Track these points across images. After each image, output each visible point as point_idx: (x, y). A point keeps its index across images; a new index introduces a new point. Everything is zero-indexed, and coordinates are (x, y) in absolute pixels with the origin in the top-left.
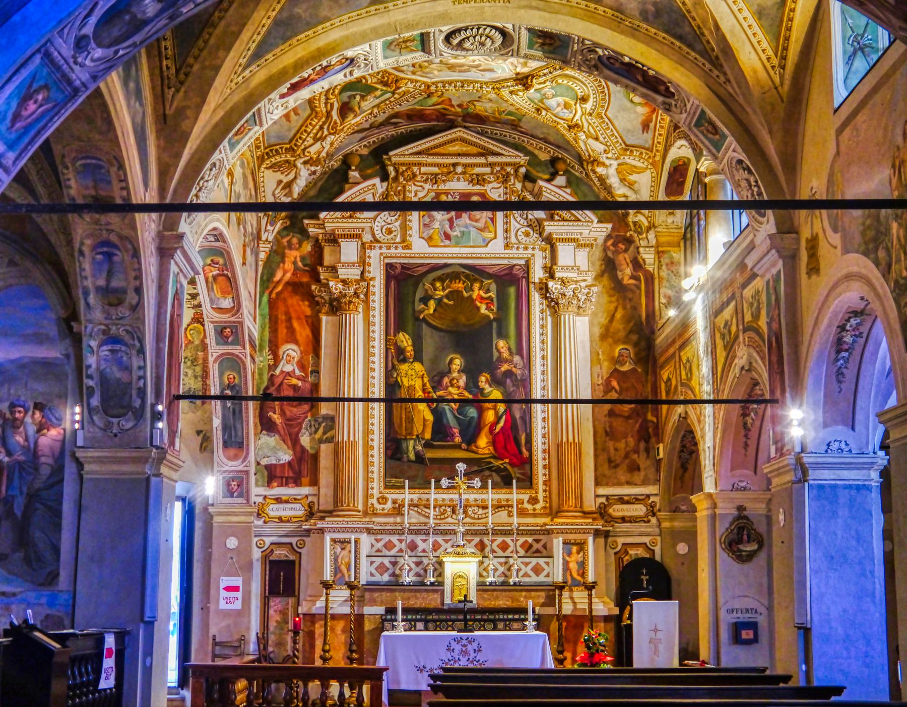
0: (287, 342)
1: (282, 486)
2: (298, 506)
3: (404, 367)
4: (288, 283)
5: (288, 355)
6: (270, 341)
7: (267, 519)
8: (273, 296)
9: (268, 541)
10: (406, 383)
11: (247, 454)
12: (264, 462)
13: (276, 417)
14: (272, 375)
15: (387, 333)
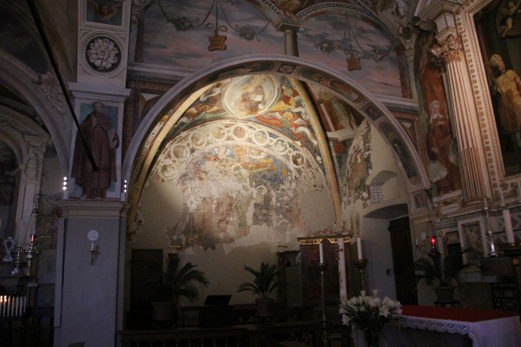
0: (432, 101)
1: (445, 193)
2: (456, 205)
3: (500, 80)
4: (426, 66)
5: (434, 108)
6: (424, 105)
7: (442, 217)
8: (421, 78)
9: (445, 231)
10: (504, 89)
11: (420, 178)
12: (434, 180)
13: (435, 150)
14: (429, 124)
15: (484, 62)
